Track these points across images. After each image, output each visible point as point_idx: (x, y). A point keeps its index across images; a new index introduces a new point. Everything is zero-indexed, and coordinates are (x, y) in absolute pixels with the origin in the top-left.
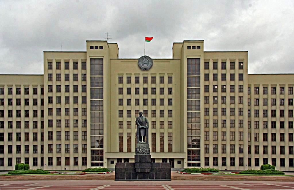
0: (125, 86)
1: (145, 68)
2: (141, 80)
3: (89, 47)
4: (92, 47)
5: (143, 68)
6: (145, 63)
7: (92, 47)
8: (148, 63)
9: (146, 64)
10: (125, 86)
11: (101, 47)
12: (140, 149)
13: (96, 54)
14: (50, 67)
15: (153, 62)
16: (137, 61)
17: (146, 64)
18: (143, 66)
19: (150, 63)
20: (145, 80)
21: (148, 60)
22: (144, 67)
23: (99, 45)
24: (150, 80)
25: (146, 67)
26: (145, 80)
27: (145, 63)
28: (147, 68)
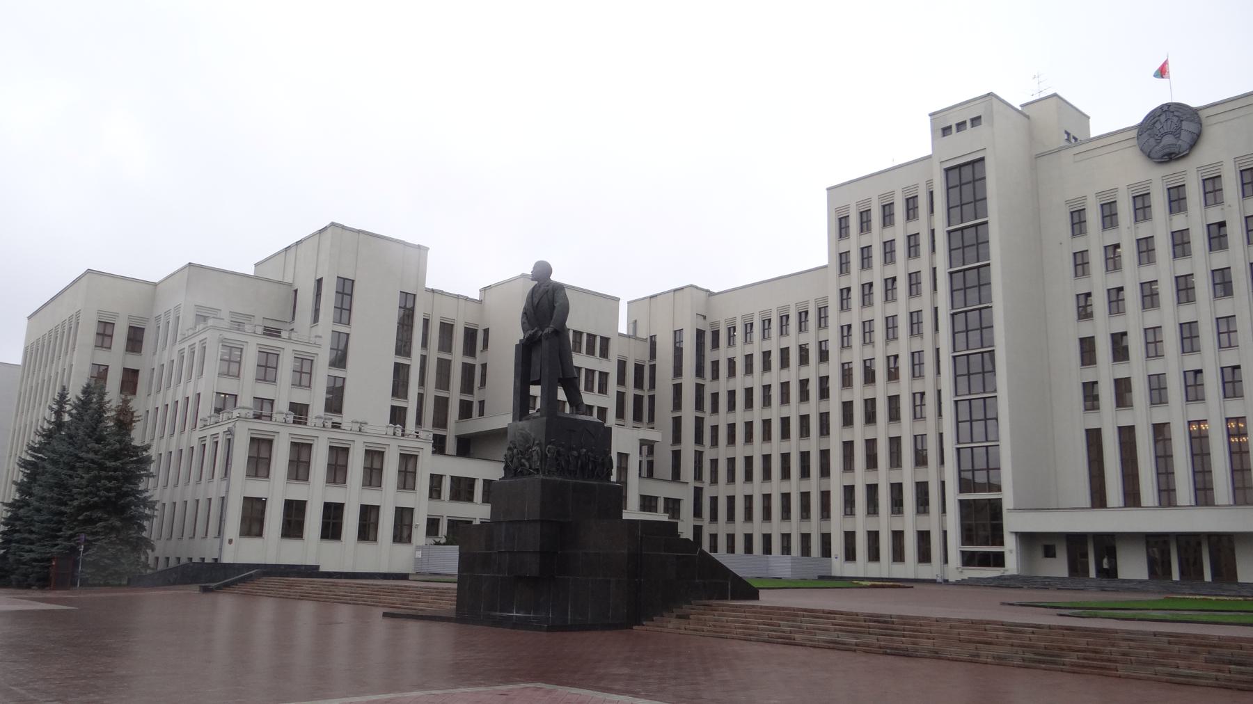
0: (1095, 240)
1: (1167, 151)
2: (1159, 202)
3: (940, 132)
4: (946, 131)
5: (1160, 154)
6: (1167, 133)
7: (946, 131)
8: (1180, 128)
9: (1171, 133)
10: (1095, 240)
11: (976, 121)
12: (515, 451)
13: (962, 147)
14: (842, 227)
15: (1204, 121)
16: (1134, 133)
17: (1171, 133)
18: (1157, 148)
19: (1185, 125)
20: (1177, 199)
21: (1175, 119)
22: (1164, 148)
23: (967, 116)
24: (1194, 194)
25: (1170, 146)
26: (1177, 199)
27: (1167, 133)
28: (1176, 150)
